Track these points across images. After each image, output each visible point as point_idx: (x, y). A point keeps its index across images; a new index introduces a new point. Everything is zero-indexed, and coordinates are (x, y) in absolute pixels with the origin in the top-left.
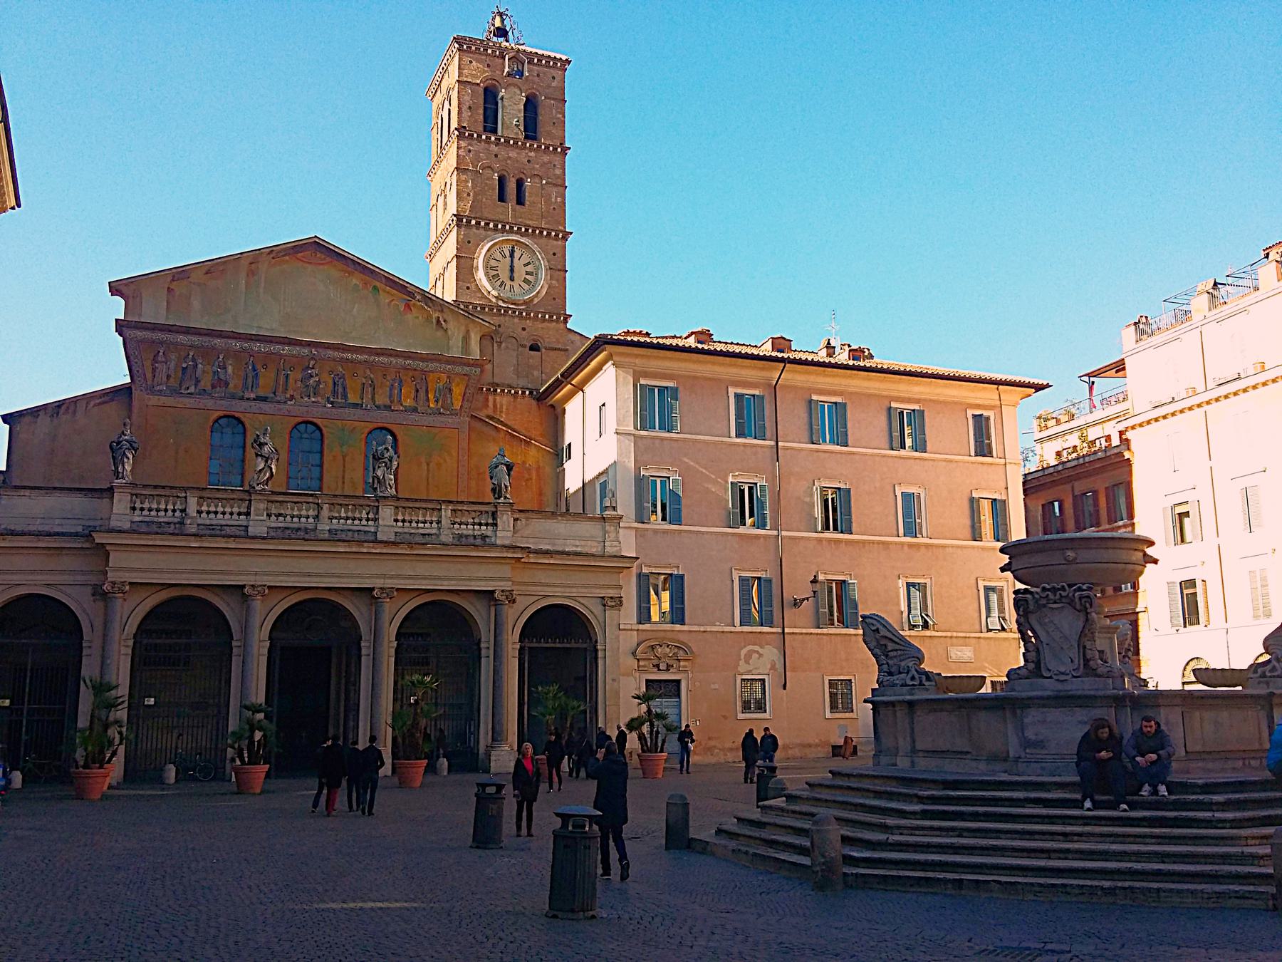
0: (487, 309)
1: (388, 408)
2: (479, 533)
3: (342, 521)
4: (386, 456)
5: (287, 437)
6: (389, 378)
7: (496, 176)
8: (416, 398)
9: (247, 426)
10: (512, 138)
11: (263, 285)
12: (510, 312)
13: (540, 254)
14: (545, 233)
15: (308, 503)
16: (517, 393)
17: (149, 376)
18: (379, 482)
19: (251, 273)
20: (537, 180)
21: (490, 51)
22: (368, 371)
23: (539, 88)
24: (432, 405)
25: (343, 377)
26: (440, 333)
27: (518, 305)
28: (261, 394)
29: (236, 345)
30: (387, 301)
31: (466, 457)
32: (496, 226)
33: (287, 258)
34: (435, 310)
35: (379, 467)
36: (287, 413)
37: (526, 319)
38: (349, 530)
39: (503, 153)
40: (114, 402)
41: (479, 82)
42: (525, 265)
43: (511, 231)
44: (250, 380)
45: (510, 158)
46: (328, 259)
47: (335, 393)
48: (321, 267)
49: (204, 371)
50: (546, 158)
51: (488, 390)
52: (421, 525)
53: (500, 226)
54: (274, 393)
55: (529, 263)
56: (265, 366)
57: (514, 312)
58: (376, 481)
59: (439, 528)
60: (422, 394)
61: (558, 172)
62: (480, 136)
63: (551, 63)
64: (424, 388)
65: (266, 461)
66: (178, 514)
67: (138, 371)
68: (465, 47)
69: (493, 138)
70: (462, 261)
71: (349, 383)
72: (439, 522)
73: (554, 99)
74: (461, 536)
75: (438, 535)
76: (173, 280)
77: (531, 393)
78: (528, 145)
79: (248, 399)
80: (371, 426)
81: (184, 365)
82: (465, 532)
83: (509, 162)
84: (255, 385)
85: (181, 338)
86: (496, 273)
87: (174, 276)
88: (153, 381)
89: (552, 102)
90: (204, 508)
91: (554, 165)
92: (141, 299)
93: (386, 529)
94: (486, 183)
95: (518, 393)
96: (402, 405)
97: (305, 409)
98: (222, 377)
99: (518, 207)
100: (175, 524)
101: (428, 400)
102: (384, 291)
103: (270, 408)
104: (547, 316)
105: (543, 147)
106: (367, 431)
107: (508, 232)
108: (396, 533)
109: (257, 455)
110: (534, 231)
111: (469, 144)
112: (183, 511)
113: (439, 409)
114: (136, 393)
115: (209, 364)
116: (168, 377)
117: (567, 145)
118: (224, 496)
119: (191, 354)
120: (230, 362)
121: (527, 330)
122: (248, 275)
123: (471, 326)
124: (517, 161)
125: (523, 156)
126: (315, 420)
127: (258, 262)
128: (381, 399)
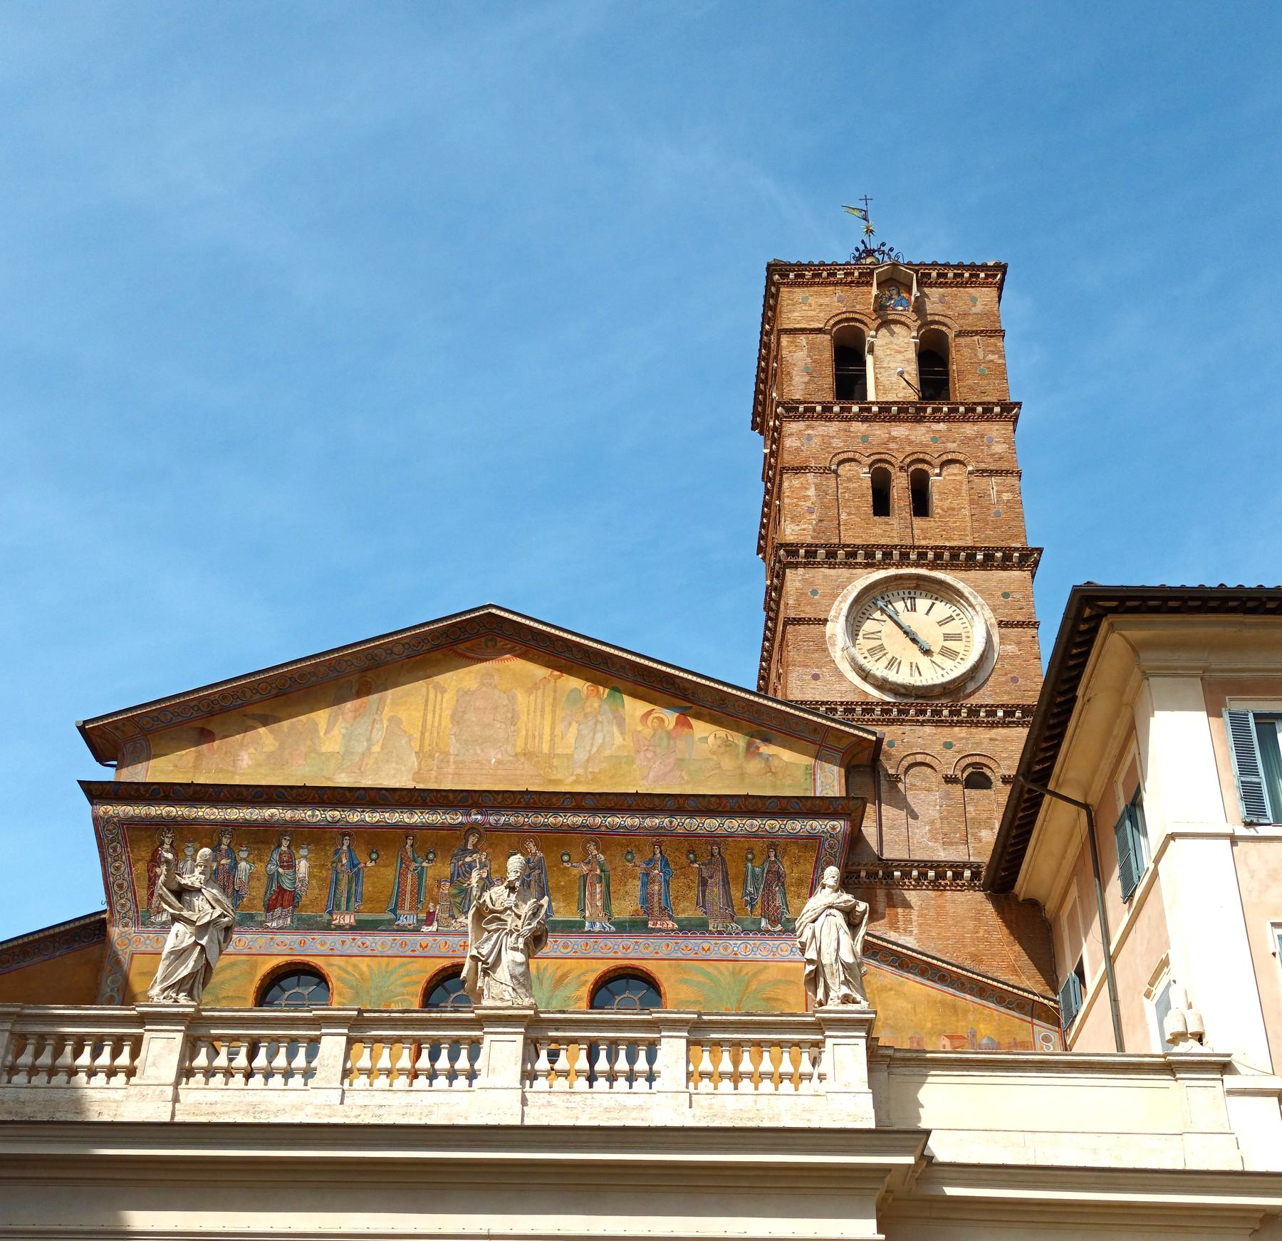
7: (864, 475)
8: (702, 903)
9: (334, 982)
10: (895, 403)
12: (912, 712)
13: (975, 597)
14: (980, 557)
16: (940, 876)
17: (142, 893)
20: (954, 469)
21: (840, 275)
22: (592, 847)
23: (947, 320)
27: (931, 698)
28: (365, 916)
32: (870, 555)
33: (436, 655)
37: (952, 724)
39: (879, 431)
41: (821, 326)
42: (941, 623)
43: (904, 559)
44: (343, 886)
45: (893, 439)
49: (251, 876)
50: (969, 429)
51: (872, 875)
53: (879, 555)
54: (394, 911)
55: (951, 618)
57: (923, 712)
60: (715, 892)
61: (999, 448)
62: (828, 409)
63: (967, 275)
64: (719, 876)
68: (792, 276)
69: (855, 409)
73: (977, 333)
77: (975, 875)
78: (929, 410)
79: (340, 928)
80: (602, 967)
83: (892, 445)
86: (876, 643)
89: (976, 338)
91: (991, 440)
94: (847, 488)
95: (944, 878)
98: (287, 885)
99: (919, 522)
101: (729, 902)
104: (1000, 713)
105: (962, 409)
106: (592, 978)
107: (898, 566)
110: (954, 556)
111: (808, 427)
115: (261, 860)
117: (1013, 399)
120: (304, 852)
121: (958, 746)
124: (910, 443)
125: (920, 434)
128: (626, 907)
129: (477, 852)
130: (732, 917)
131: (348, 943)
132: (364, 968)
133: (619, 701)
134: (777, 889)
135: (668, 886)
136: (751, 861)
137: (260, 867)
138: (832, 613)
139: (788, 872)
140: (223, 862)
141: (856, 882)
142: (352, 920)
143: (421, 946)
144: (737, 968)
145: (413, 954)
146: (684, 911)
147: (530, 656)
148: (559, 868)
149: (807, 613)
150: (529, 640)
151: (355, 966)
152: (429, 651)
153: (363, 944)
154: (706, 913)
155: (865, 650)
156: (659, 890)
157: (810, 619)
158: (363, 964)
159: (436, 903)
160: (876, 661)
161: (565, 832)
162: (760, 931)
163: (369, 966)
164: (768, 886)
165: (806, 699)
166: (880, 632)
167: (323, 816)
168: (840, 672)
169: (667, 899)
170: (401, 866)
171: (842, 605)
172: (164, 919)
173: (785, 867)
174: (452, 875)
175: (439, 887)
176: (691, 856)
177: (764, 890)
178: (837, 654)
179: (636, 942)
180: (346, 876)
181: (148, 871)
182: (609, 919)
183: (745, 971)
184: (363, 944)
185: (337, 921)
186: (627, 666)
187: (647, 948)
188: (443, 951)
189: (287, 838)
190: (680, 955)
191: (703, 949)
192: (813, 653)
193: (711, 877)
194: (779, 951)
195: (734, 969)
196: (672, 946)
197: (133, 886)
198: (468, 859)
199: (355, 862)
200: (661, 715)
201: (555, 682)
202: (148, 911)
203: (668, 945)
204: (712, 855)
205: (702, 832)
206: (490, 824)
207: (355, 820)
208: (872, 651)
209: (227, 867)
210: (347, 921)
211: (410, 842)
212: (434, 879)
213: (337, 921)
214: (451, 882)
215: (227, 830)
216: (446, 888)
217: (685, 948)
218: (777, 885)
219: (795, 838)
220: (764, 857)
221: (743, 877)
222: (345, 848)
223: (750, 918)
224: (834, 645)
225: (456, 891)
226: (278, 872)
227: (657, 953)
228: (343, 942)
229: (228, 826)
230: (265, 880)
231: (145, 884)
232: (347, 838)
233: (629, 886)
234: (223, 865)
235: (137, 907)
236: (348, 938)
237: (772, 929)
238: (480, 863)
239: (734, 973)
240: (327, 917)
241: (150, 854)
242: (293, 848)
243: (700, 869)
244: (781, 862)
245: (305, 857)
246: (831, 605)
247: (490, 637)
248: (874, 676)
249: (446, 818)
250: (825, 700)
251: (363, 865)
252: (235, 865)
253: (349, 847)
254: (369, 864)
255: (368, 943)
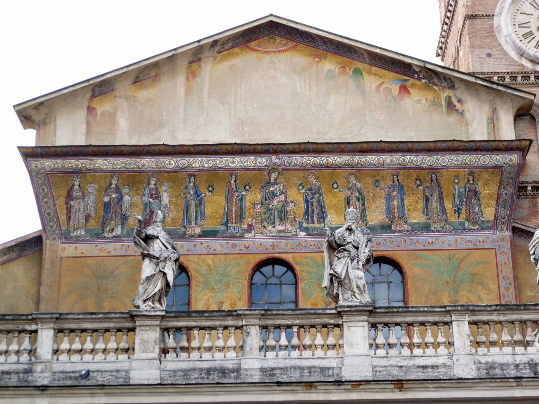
0: (519, 78)
1: (386, 228)
2: (525, 359)
3: (282, 354)
4: (349, 240)
5: (246, 283)
6: (382, 185)
8: (426, 211)
11: (206, 88)
15: (226, 328)
17: (63, 218)
18: (340, 283)
19: (192, 75)
22: (352, 178)
24: (451, 219)
25: (318, 191)
26: (453, 119)
29: (170, 163)
30: (374, 85)
31: (512, 290)
33: (237, 50)
34: (444, 88)
35: (339, 259)
36: (244, 250)
38: (295, 368)
40: (21, 259)
44: (192, 211)
46: (291, 44)
47: (309, 215)
48: (283, 55)
49: (132, 204)
52: (417, 352)
54: (226, 224)
56: (211, 187)
58: (336, 284)
59: (450, 356)
60: (434, 203)
64: (436, 194)
65: (157, 265)
66: (25, 358)
67: (49, 214)
70: (478, 22)
71: (328, 200)
72: (450, 344)
74: (491, 366)
75: (450, 367)
76: (93, 96)
79: (192, 236)
81: (106, 199)
82: (499, 359)
84: (199, 215)
85: (100, 163)
86: (527, 30)
87: (93, 90)
88: (68, 223)
90: (65, 346)
92: (55, 126)
93: (356, 361)
96: (406, 222)
97: (269, 242)
100: (18, 373)
101: (444, 211)
102: (370, 73)
103: (221, 245)
108: (374, 367)
109: (144, 256)
112: (32, 352)
113: (462, 224)
114: (47, 243)
115: (138, 194)
116: (87, 218)
118: (95, 325)
119: (114, 182)
120: (165, 188)
122: (188, 79)
123: (499, 104)
126: (283, 256)
127: (200, 59)
129: (277, 184)
130: (446, 221)
131: (198, 246)
132: (210, 262)
133: (361, 79)
134: (475, 201)
135: (403, 202)
136: (457, 184)
137: (137, 199)
138: (497, 11)
139: (481, 191)
140: (114, 196)
141: (525, 194)
142: (200, 231)
143: (245, 246)
144: (452, 256)
145: (240, 252)
146: (414, 218)
147: (298, 48)
148: (331, 193)
149: (480, 11)
150: (298, 38)
151: (204, 261)
152: (232, 47)
153: (208, 246)
154: (429, 219)
155: (520, 36)
156: (398, 205)
157: (483, 15)
158: (209, 260)
159: (253, 218)
160: (529, 42)
161: (334, 169)
162: (464, 229)
163: (213, 260)
164: (469, 200)
165: (483, 71)
166: (529, 22)
167: (177, 164)
168: (505, 51)
169: (403, 211)
170: (228, 195)
171: (504, 4)
172: (78, 234)
173: (480, 186)
174: (262, 200)
175: (254, 208)
176: (418, 182)
177: (466, 203)
178: (502, 40)
179: (385, 240)
180: (193, 203)
181: (66, 203)
182: (366, 225)
183: (457, 256)
184: (208, 246)
185: (190, 232)
186: (364, 53)
187: (391, 243)
188: (260, 250)
189: (154, 179)
190: (412, 247)
191: (429, 243)
192: (486, 39)
193: (432, 195)
194: (478, 243)
195: (449, 255)
196: (408, 241)
197: (57, 213)
198: (271, 189)
199: (199, 193)
200: (389, 86)
201: (317, 66)
202: (68, 229)
203: (405, 241)
204: (432, 181)
205: (424, 166)
206: (285, 166)
207: (197, 166)
208: (525, 36)
209: (116, 199)
210: (196, 232)
211: (233, 179)
212: (250, 202)
213: (190, 232)
214: (262, 204)
215: (115, 175)
216: (259, 208)
217: (416, 242)
218: (475, 199)
219: (485, 168)
220: (466, 181)
221: (452, 194)
222: (191, 184)
223: (458, 221)
224: (500, 32)
225: (265, 210)
226: (149, 201)
227: (399, 246)
228: (195, 246)
229: (115, 172)
230: (141, 207)
231: (65, 211)
232: (193, 177)
233: (378, 203)
234: (114, 198)
235: (60, 227)
236: (198, 242)
237: (472, 228)
238: (280, 191)
239: (450, 258)
240: (183, 229)
241: (66, 193)
242: (157, 185)
243: (424, 191)
244: (477, 184)
245: (166, 191)
246: (496, 5)
247: (271, 36)
248: (528, 54)
249: (256, 163)
250: (497, 71)
251: (203, 195)
252: (120, 199)
253: (194, 183)
254: (208, 194)
255: (211, 246)
